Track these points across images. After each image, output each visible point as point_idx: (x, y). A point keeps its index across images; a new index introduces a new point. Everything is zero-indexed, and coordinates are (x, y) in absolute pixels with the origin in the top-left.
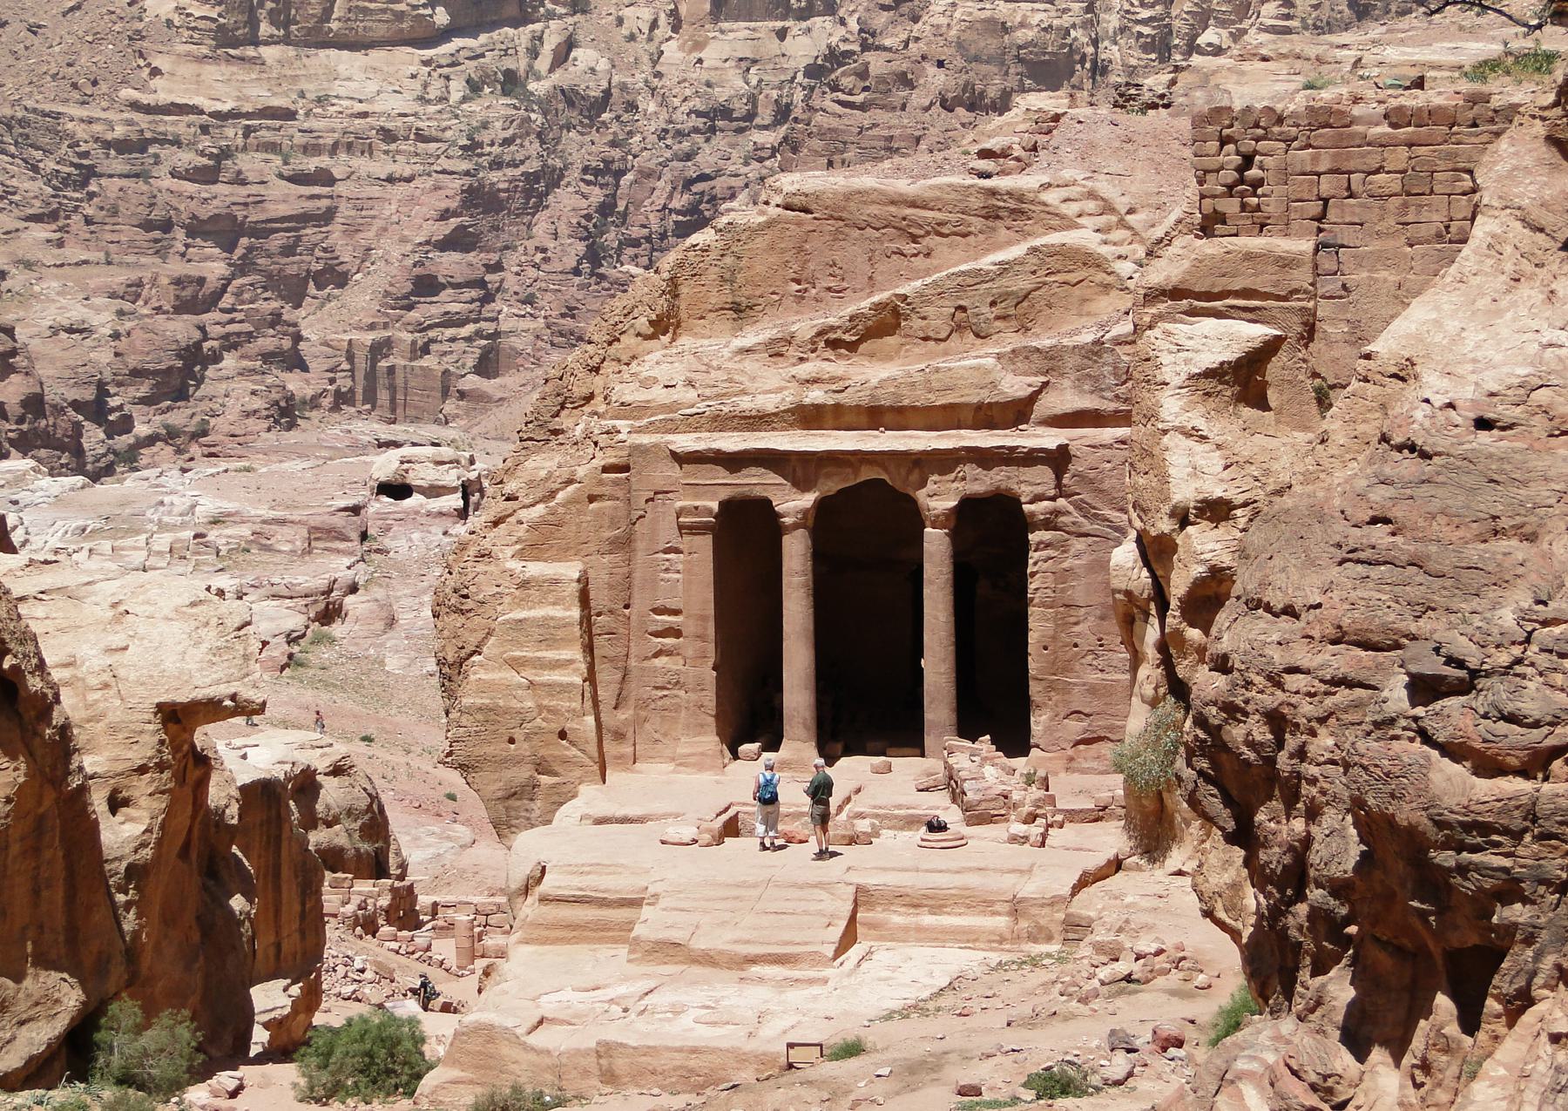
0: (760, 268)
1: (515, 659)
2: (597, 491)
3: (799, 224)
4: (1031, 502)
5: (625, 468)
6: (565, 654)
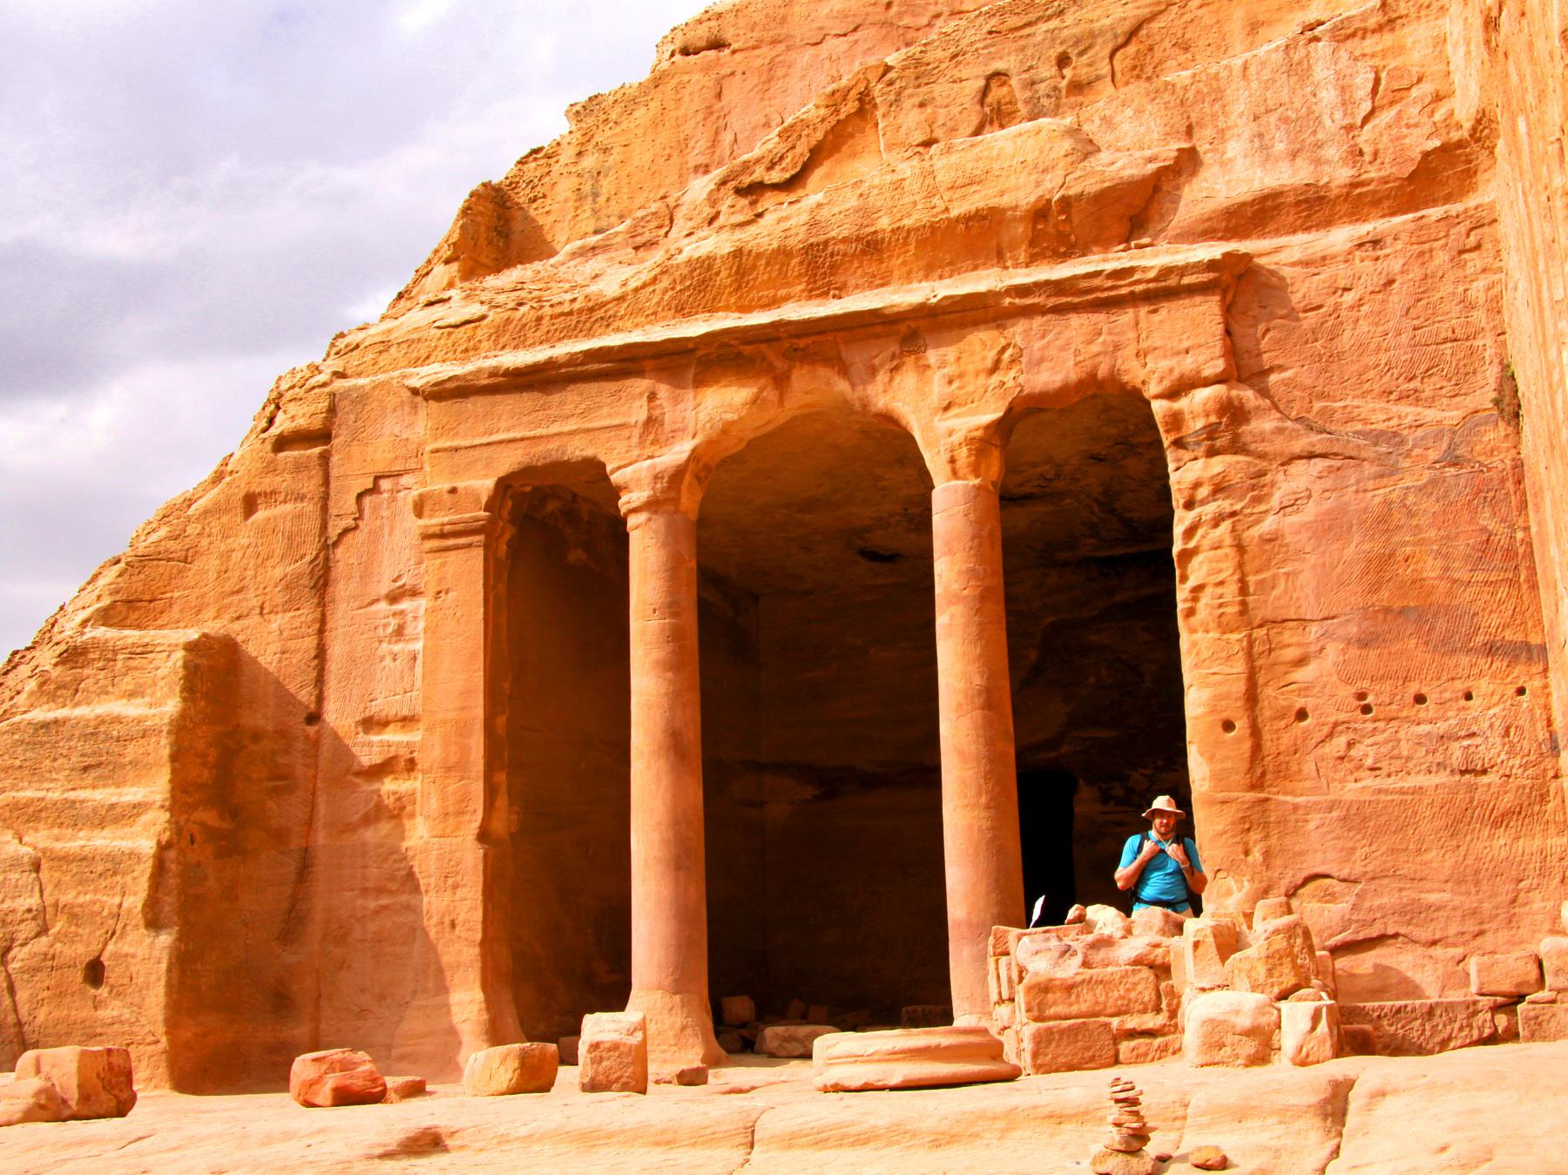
0: (641, 156)
1: (15, 806)
2: (267, 483)
3: (706, 69)
4: (1173, 394)
5: (323, 436)
6: (132, 794)
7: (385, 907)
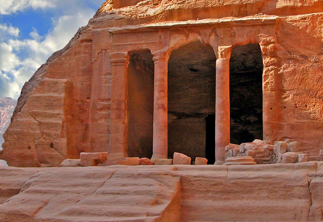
1: (33, 113)
6: (56, 112)
7: (103, 136)
